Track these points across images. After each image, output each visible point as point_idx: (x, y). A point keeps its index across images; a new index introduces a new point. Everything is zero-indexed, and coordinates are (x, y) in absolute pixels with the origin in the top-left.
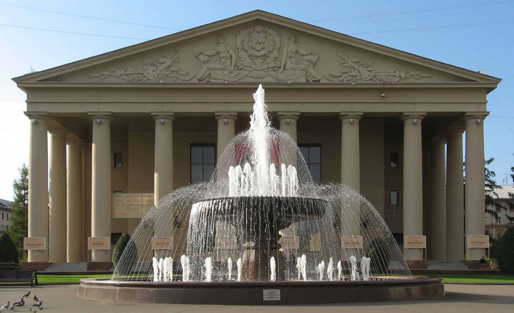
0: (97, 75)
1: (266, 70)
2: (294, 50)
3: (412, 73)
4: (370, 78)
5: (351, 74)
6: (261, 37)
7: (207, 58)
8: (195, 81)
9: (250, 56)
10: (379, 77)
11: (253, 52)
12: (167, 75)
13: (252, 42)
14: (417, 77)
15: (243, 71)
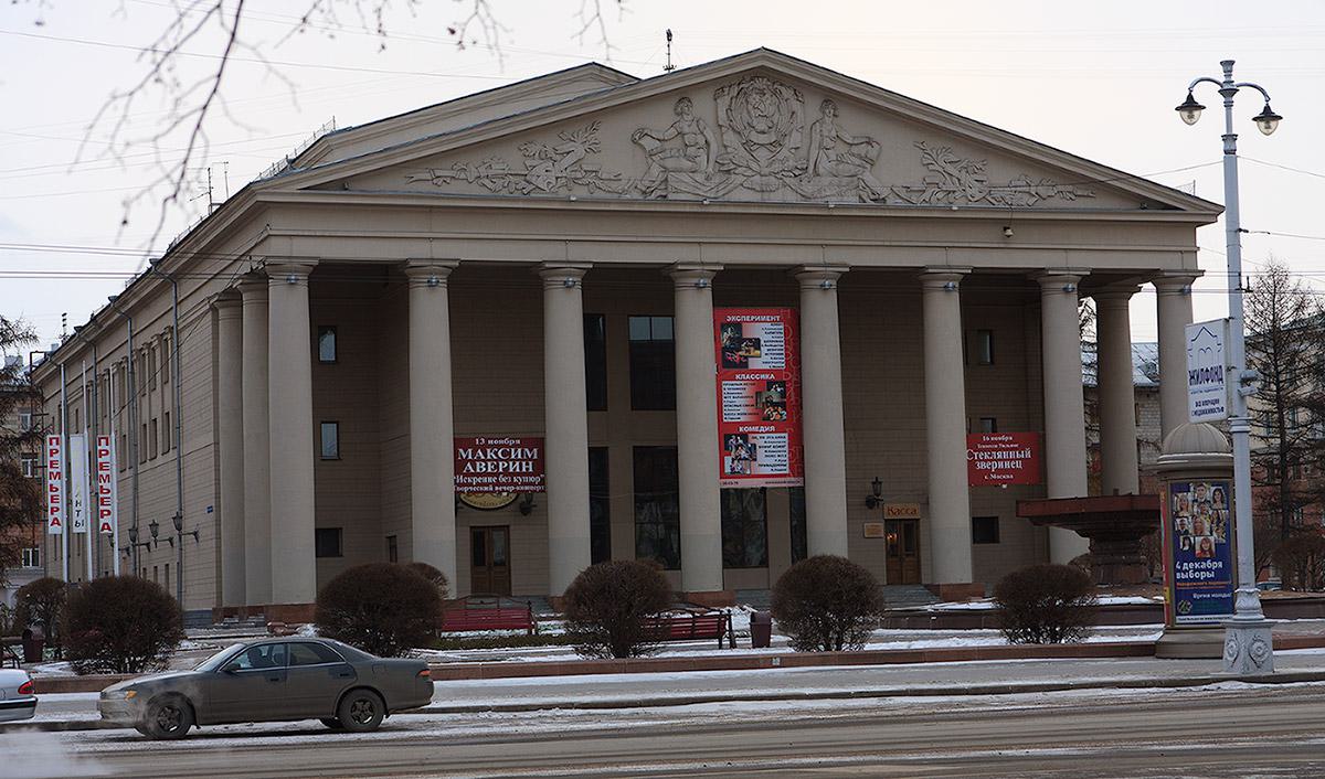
2: (834, 134)
3: (1060, 188)
4: (982, 195)
6: (768, 104)
8: (637, 195)
10: (997, 196)
11: (755, 137)
13: (749, 112)
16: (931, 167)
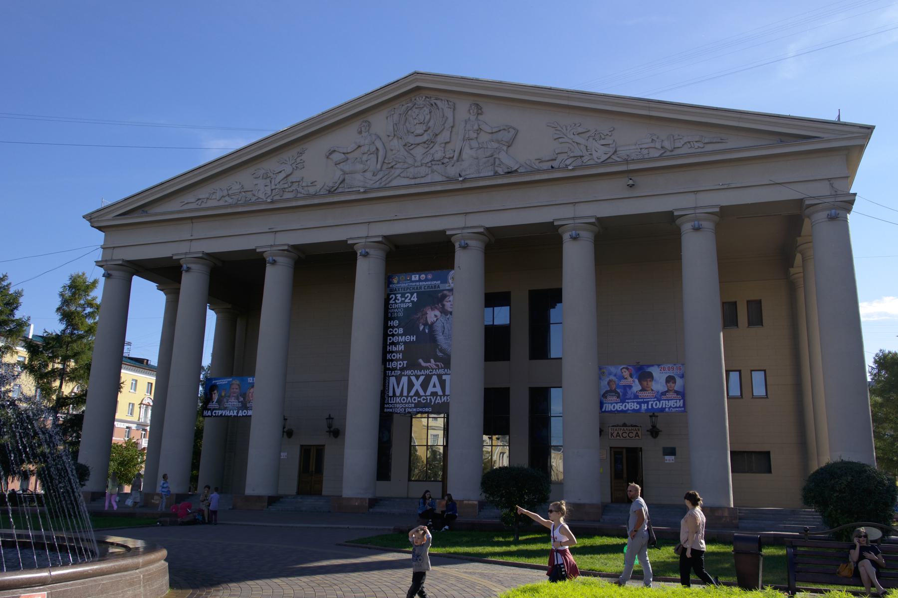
0: (193, 200)
1: (430, 165)
2: (476, 127)
5: (572, 155)
7: (343, 156)
9: (405, 145)
11: (411, 139)
12: (284, 190)
14: (697, 145)
15: (393, 171)
16: (561, 140)
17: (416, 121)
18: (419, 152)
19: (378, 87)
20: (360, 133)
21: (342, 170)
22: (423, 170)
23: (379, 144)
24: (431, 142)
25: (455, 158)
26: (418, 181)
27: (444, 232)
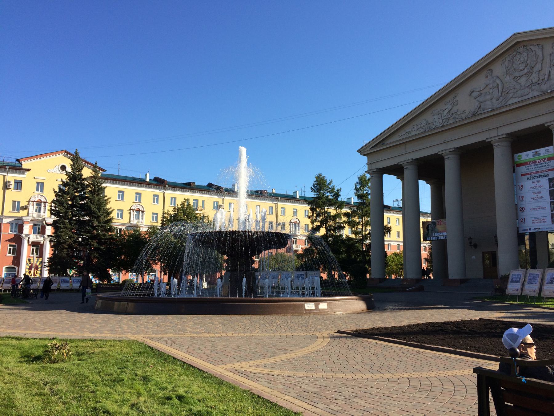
1: (530, 86)
7: (478, 93)
11: (517, 74)
12: (448, 119)
17: (519, 63)
18: (523, 81)
19: (503, 42)
20: (487, 77)
21: (479, 101)
22: (527, 91)
23: (498, 82)
24: (530, 73)
25: (546, 79)
26: (524, 98)
27: (543, 125)
